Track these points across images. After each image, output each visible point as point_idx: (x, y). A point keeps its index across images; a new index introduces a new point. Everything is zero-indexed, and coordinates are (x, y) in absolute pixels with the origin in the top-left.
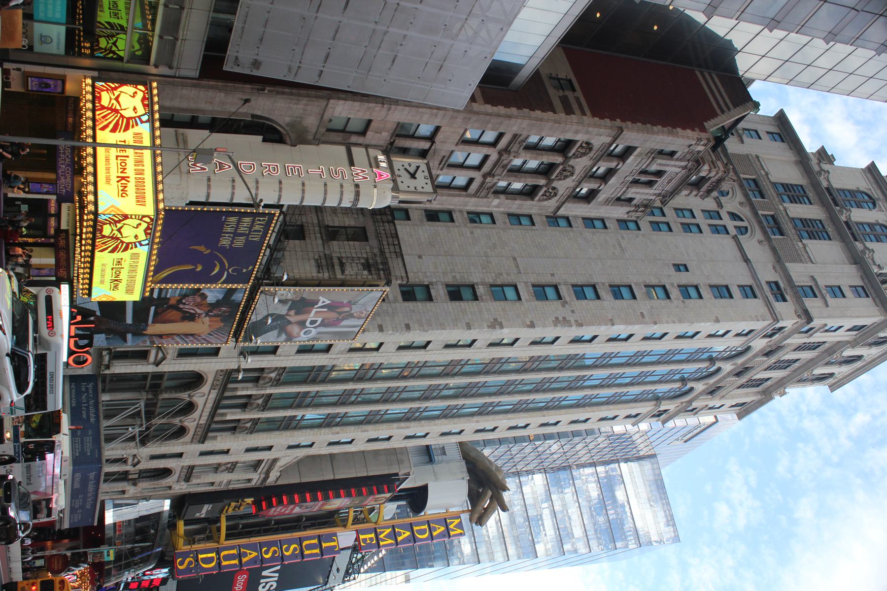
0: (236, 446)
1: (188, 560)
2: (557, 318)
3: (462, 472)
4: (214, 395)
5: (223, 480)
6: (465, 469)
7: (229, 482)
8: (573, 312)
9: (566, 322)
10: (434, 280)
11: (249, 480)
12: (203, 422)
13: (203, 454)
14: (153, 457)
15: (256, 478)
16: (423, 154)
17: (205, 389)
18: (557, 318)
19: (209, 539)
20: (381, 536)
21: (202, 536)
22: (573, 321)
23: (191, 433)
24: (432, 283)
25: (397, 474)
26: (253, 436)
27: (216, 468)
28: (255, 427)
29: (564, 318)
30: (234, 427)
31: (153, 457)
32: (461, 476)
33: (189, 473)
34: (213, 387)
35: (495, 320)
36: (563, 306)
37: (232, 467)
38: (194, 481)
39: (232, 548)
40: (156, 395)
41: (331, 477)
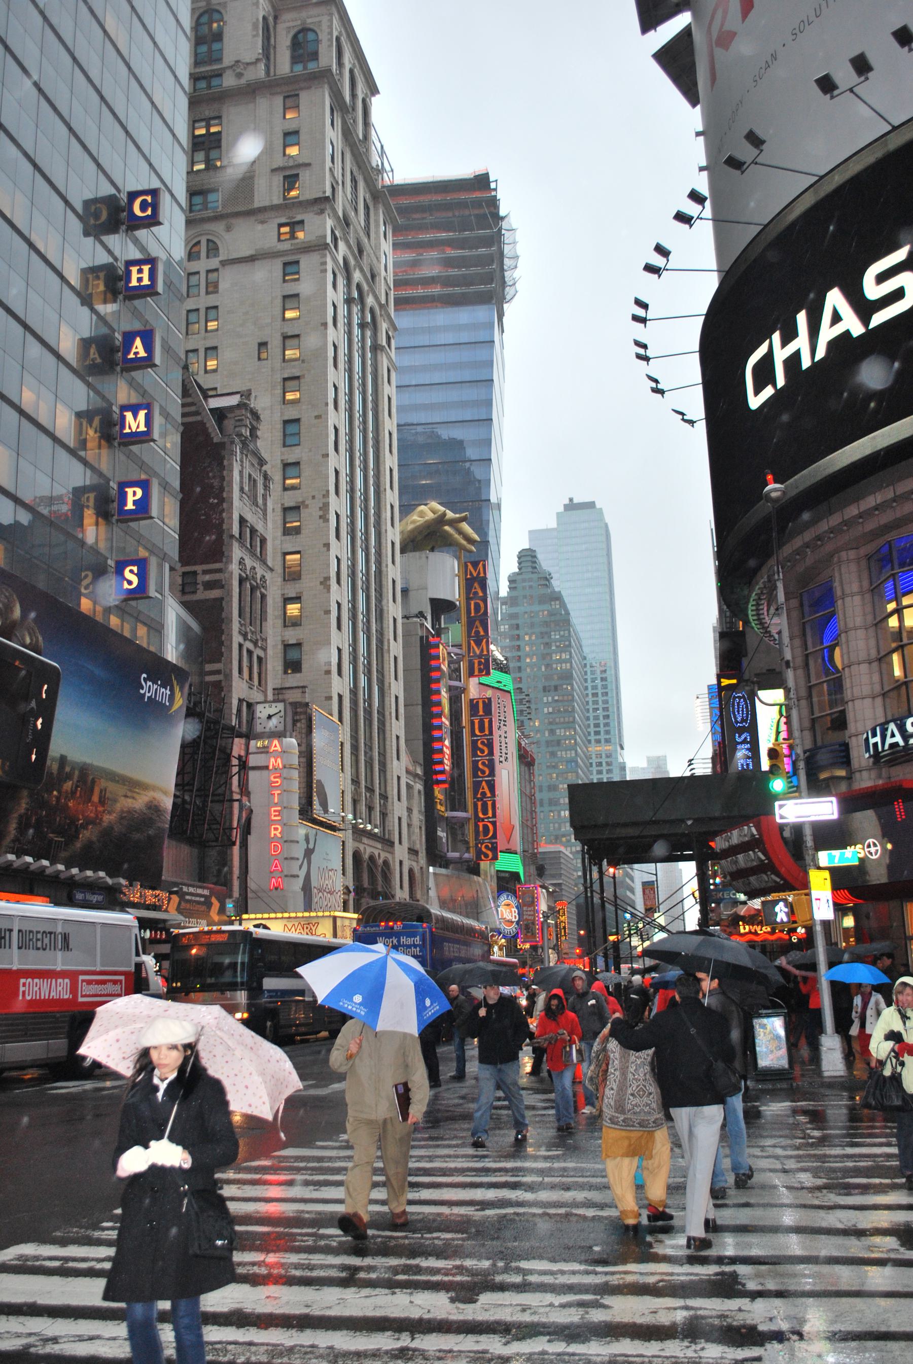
0: (398, 809)
1: (484, 850)
2: (321, 517)
3: (420, 558)
4: (365, 840)
5: (418, 818)
6: (417, 554)
7: (420, 811)
8: (313, 497)
9: (325, 507)
10: (279, 638)
11: (419, 792)
12: (379, 846)
13: (400, 843)
14: (401, 887)
15: (419, 786)
16: (250, 706)
17: (361, 847)
18: (321, 517)
19: (462, 826)
20: (478, 652)
21: (459, 832)
22: (324, 500)
23: (388, 855)
24: (283, 641)
25: (422, 638)
26: (390, 797)
27: (409, 825)
28: (384, 797)
29: (320, 509)
30: (384, 815)
31: (401, 887)
32: (424, 559)
33: (413, 852)
34: (360, 842)
35: (321, 583)
36: (307, 506)
37: (410, 810)
38: (417, 847)
39: (475, 806)
40: (365, 889)
41: (420, 708)
